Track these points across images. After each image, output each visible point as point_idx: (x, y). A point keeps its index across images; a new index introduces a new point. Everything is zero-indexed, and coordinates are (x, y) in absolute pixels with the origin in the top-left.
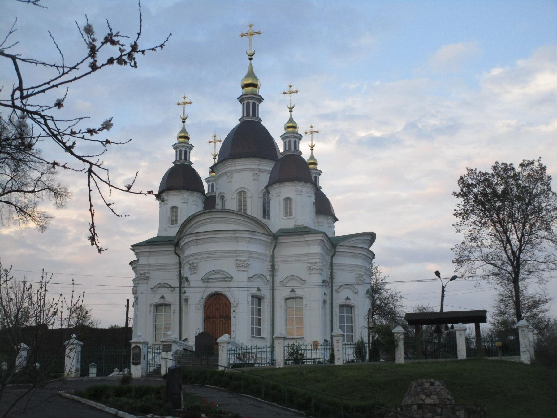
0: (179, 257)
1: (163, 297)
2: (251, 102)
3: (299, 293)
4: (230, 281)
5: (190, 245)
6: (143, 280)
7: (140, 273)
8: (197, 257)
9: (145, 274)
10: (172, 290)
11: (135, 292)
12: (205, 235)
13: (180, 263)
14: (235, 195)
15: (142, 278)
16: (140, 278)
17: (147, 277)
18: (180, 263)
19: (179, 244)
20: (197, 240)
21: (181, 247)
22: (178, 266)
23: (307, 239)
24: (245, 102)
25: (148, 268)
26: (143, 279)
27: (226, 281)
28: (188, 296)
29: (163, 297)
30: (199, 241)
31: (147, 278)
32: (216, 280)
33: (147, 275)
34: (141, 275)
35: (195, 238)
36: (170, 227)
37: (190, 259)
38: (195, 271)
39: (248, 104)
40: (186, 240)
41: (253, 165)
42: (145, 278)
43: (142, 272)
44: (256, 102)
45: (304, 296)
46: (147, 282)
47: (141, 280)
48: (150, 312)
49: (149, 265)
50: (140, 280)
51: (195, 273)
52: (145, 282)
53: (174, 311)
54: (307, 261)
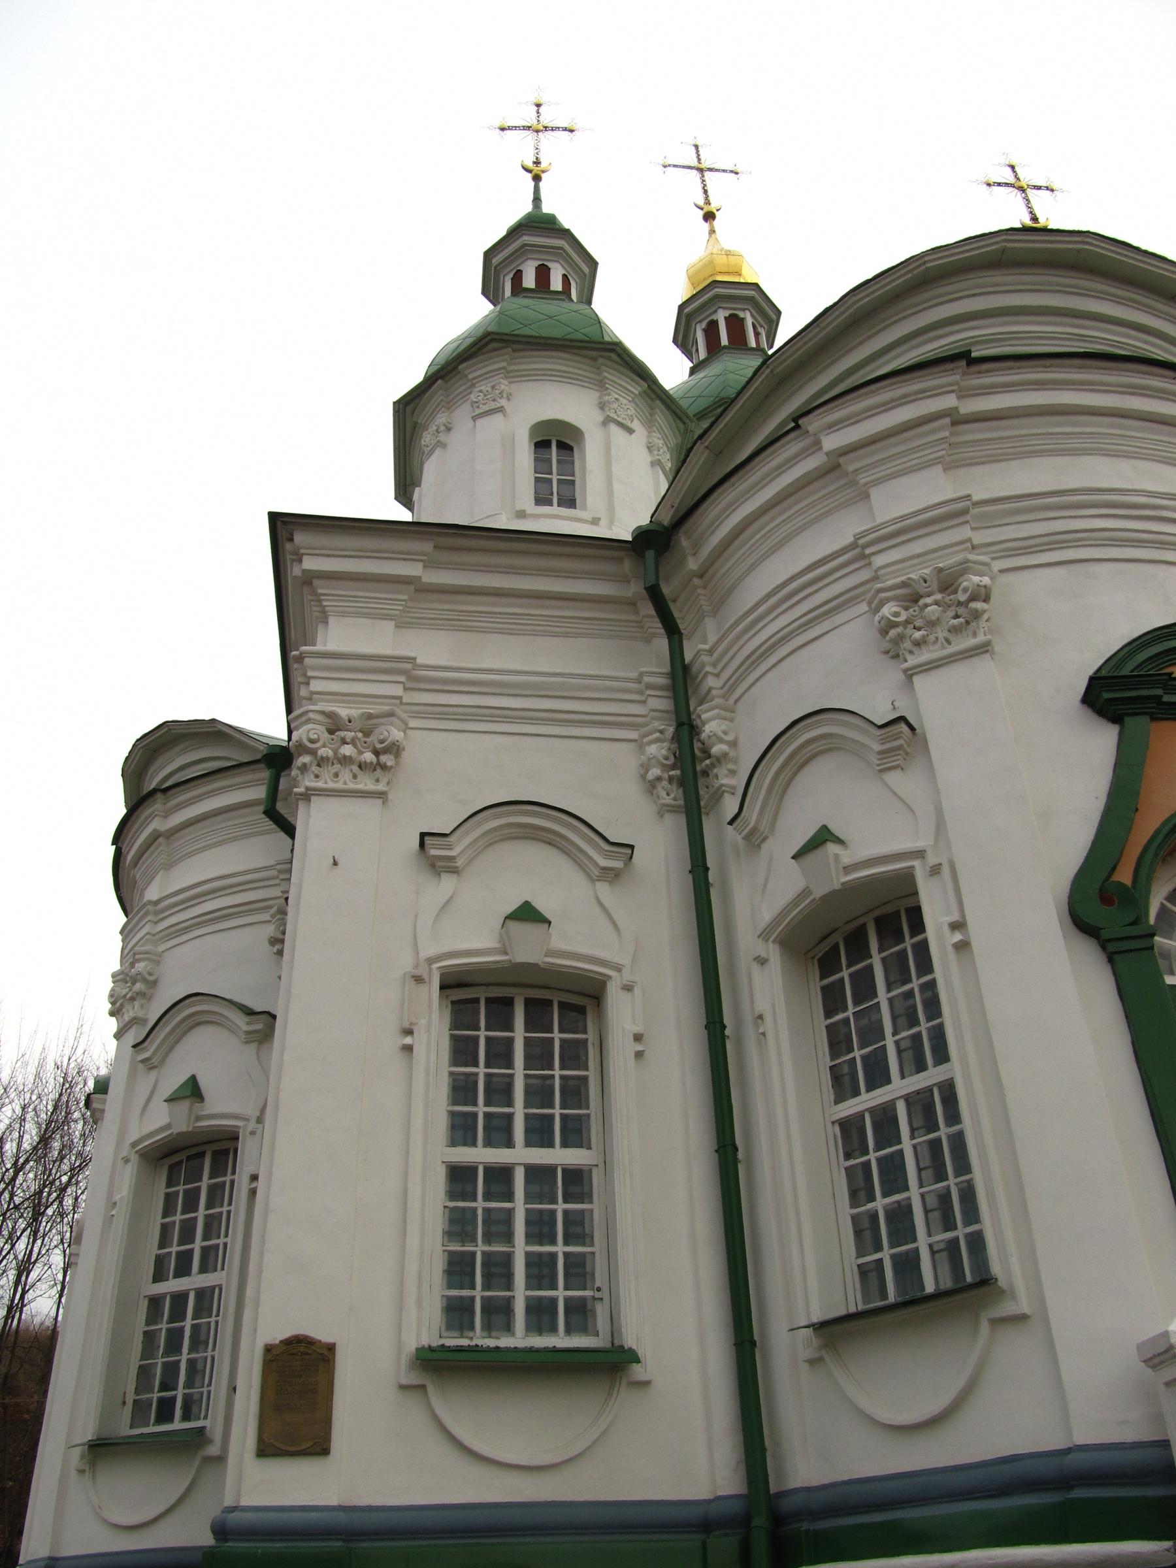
0: (672, 630)
1: (527, 914)
5: (863, 479)
6: (346, 775)
7: (331, 715)
8: (978, 538)
9: (367, 733)
10: (618, 864)
11: (139, 986)
12: (1041, 385)
15: (347, 750)
16: (324, 752)
17: (395, 749)
19: (684, 542)
20: (958, 420)
21: (692, 564)
22: (661, 703)
24: (721, 317)
25: (398, 690)
26: (346, 761)
28: (920, 854)
30: (971, 433)
31: (387, 759)
33: (396, 734)
34: (331, 732)
35: (949, 402)
37: (879, 561)
38: (981, 638)
39: (735, 324)
40: (831, 442)
42: (369, 757)
43: (344, 712)
44: (761, 330)
46: (380, 787)
47: (327, 773)
48: (409, 1032)
50: (322, 762)
51: (983, 649)
52: (366, 783)
53: (638, 1038)
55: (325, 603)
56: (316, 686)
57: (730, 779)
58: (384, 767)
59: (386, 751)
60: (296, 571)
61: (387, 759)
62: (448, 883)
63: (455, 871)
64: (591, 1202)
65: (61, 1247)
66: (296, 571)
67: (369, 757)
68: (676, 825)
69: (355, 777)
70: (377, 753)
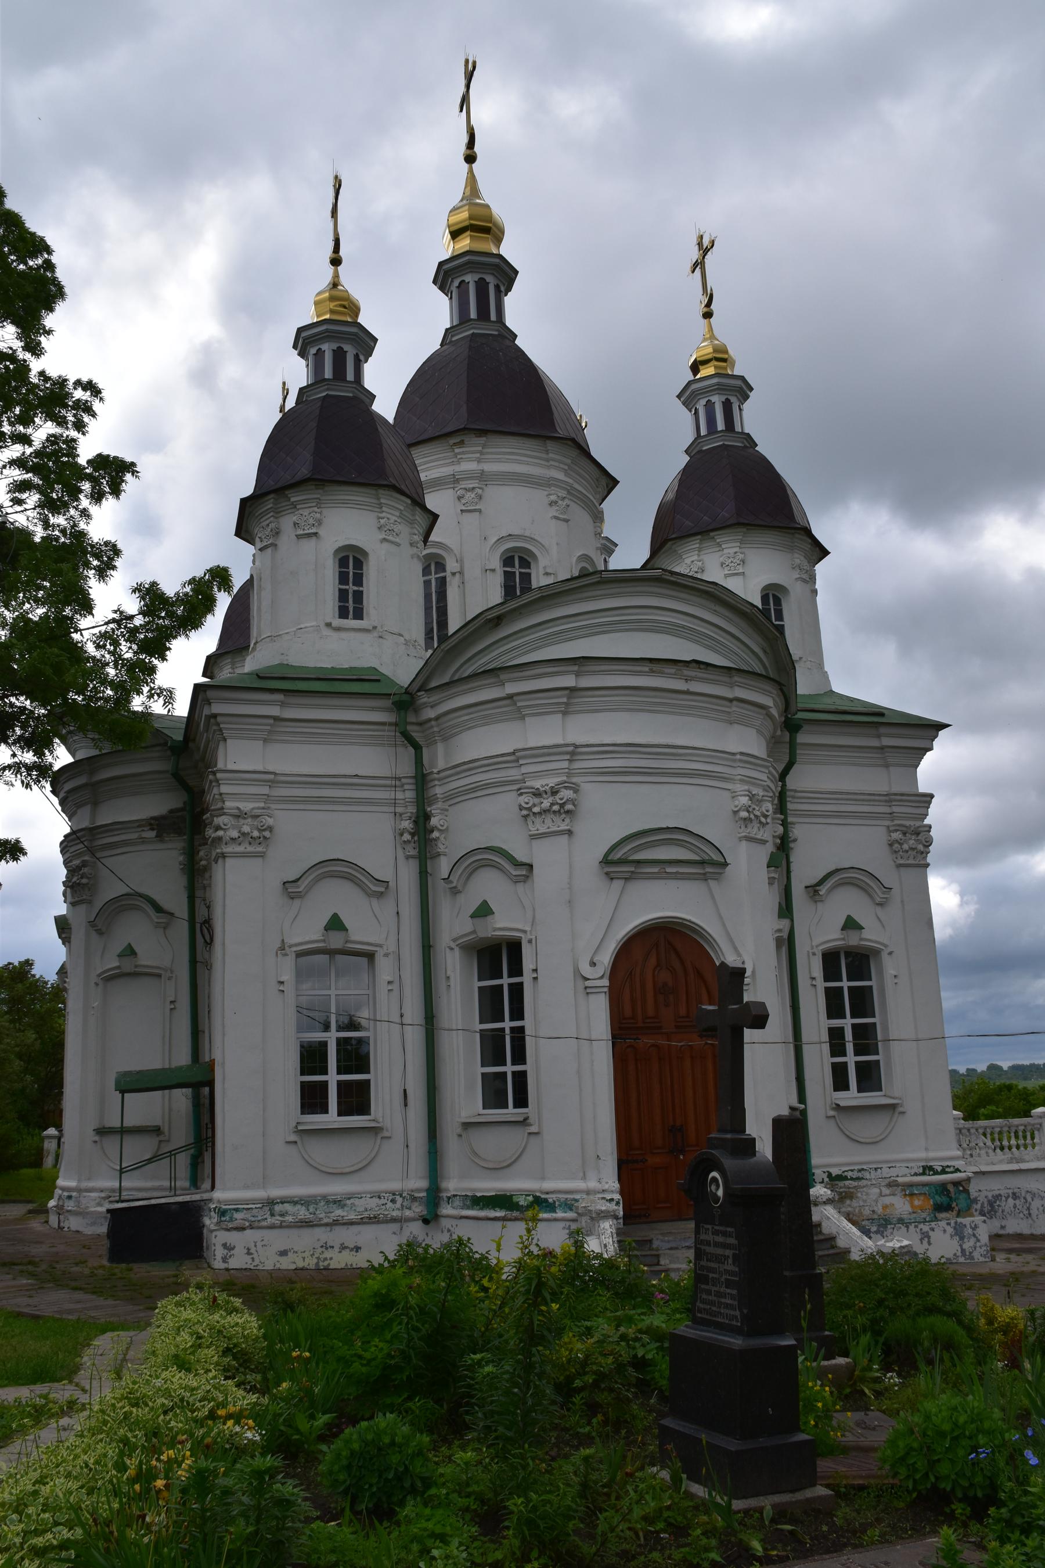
2: (470, 278)
3: (871, 935)
4: (717, 877)
13: (422, 780)
14: (496, 563)
17: (270, 829)
18: (422, 780)
23: (886, 741)
27: (705, 878)
29: (335, 924)
32: (664, 869)
33: (270, 821)
36: (338, 629)
41: (549, 467)
45: (886, 946)
49: (273, 779)
54: (887, 823)
55: (222, 726)
56: (224, 789)
57: (444, 866)
58: (265, 838)
59: (264, 830)
60: (206, 711)
61: (267, 834)
62: (297, 902)
63: (300, 897)
64: (368, 1072)
65: (405, 1319)
66: (206, 711)
67: (256, 834)
68: (413, 866)
69: (250, 844)
70: (260, 831)
